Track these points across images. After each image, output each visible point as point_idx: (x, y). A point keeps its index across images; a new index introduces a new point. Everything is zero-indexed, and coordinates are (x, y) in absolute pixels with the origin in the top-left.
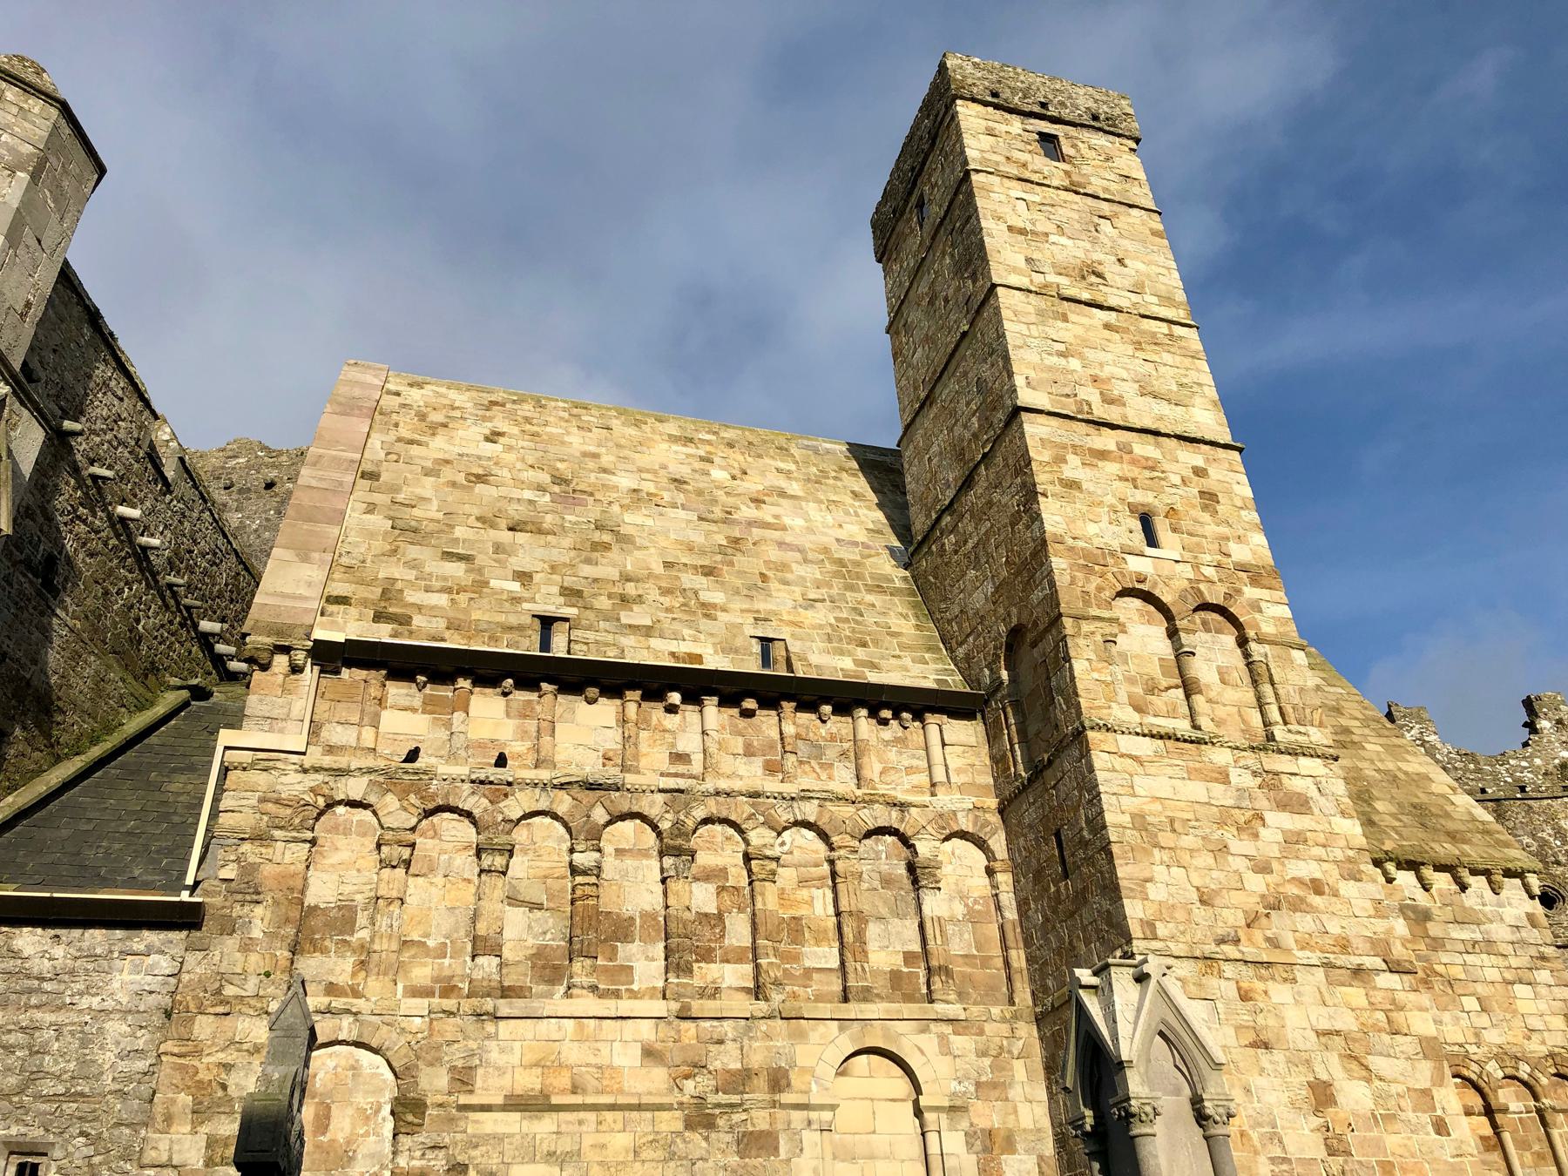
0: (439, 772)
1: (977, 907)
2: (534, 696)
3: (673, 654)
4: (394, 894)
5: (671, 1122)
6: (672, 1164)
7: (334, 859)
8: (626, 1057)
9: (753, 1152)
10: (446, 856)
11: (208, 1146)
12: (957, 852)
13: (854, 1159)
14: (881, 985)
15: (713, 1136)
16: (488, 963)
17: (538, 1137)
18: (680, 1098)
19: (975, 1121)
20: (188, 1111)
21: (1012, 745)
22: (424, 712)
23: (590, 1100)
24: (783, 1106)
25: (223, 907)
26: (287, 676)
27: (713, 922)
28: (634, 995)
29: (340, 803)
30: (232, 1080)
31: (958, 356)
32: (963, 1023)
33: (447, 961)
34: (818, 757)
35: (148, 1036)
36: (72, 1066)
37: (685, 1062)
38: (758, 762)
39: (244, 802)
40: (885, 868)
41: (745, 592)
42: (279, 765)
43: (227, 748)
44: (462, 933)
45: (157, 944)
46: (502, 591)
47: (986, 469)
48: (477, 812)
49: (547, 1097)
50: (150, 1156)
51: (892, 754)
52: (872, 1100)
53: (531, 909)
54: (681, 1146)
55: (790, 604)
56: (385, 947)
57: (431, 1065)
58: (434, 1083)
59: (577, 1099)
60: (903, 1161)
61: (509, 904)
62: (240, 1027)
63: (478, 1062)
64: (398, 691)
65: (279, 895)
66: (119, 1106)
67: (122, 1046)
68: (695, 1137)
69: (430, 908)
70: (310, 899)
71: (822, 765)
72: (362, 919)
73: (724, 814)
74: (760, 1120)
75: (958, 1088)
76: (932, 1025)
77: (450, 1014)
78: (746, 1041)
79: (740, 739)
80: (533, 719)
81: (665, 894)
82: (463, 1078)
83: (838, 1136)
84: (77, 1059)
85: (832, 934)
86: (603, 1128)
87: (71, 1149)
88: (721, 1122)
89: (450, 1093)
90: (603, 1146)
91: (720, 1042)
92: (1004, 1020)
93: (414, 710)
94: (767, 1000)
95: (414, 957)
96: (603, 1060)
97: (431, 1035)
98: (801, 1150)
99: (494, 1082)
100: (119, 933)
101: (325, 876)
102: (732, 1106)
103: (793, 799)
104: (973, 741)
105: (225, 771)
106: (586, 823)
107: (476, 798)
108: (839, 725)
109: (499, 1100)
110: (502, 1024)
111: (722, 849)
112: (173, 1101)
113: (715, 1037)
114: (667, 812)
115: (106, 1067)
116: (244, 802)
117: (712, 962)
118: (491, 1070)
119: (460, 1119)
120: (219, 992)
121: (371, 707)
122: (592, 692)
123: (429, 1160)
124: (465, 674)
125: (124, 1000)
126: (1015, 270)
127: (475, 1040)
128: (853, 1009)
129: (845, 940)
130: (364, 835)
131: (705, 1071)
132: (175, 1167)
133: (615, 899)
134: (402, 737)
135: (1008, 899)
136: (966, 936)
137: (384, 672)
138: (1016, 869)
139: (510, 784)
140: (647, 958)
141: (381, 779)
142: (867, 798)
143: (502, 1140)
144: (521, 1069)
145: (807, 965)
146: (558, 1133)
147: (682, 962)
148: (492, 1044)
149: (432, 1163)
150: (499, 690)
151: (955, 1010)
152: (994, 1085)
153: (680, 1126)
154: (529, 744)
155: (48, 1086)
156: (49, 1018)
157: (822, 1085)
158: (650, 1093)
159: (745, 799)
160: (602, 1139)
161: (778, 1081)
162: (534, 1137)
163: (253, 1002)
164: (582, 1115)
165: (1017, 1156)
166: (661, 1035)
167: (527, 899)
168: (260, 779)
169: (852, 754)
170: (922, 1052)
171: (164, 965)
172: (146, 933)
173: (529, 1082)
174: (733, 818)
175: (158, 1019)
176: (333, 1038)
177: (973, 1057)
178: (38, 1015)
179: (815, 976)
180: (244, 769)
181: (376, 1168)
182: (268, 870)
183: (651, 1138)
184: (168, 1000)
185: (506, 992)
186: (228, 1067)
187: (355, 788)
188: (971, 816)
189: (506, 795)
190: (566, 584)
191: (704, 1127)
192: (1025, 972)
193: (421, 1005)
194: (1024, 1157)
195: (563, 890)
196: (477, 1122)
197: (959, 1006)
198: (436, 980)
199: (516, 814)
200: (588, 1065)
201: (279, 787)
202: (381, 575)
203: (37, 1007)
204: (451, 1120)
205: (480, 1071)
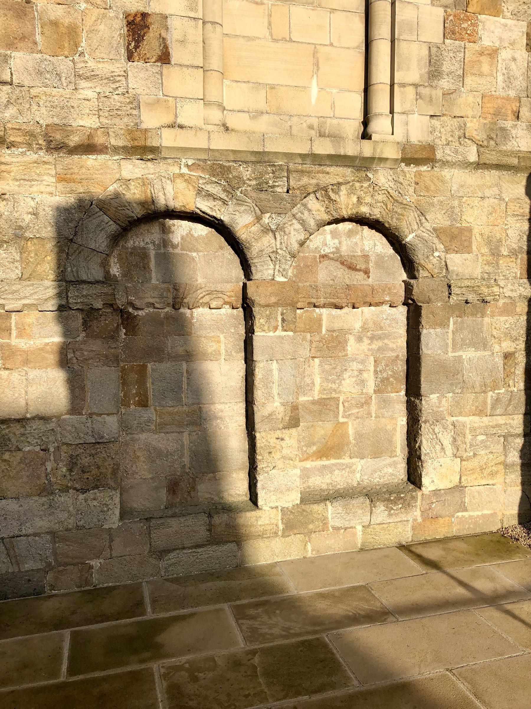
60: (333, 10)
165: (500, 19)
194: (510, 22)
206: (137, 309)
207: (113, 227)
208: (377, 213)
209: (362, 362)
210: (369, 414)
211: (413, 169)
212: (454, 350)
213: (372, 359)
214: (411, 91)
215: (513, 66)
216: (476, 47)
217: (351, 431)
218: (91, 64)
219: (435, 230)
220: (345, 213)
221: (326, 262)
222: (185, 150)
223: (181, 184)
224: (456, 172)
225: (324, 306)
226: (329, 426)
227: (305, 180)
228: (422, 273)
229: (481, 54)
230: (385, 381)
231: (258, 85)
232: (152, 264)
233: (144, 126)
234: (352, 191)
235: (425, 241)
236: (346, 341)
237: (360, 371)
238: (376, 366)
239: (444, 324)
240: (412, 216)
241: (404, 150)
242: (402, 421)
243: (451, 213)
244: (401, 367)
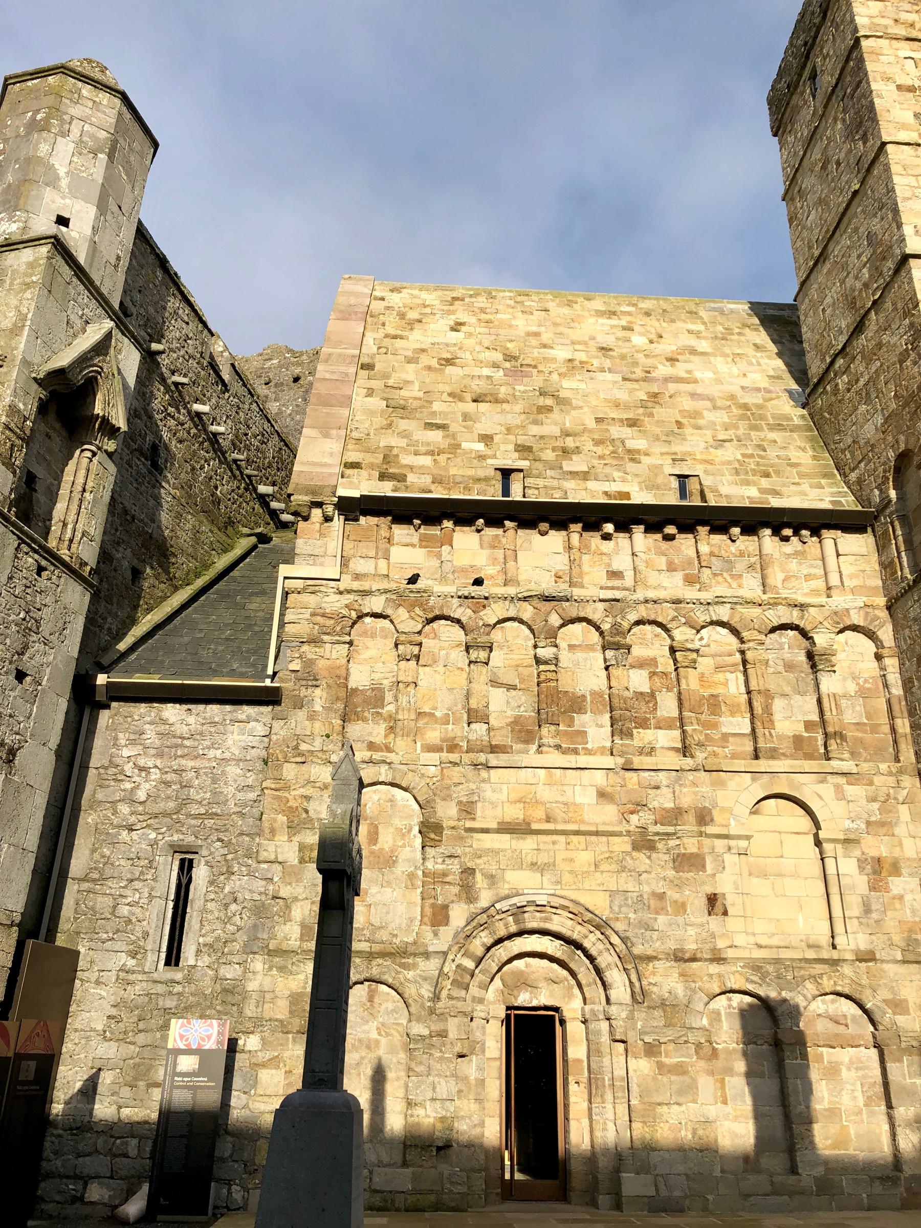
0: (435, 590)
2: (500, 531)
3: (606, 493)
4: (410, 679)
5: (622, 845)
6: (624, 874)
7: (366, 655)
8: (586, 797)
9: (686, 868)
11: (300, 851)
12: (850, 642)
13: (765, 875)
14: (785, 747)
15: (654, 855)
16: (479, 729)
18: (627, 828)
19: (866, 851)
20: (285, 827)
21: (899, 553)
23: (560, 827)
24: (707, 836)
25: (294, 690)
26: (322, 524)
27: (647, 699)
28: (589, 752)
29: (367, 615)
30: (311, 807)
31: (849, 213)
32: (856, 776)
33: (450, 727)
34: (729, 570)
35: (254, 777)
36: (208, 795)
37: (630, 802)
38: (679, 577)
39: (301, 616)
40: (787, 656)
41: (664, 438)
42: (322, 589)
43: (285, 578)
44: (460, 706)
45: (254, 715)
46: (471, 450)
47: (876, 314)
48: (464, 620)
49: (529, 824)
50: (263, 855)
51: (793, 565)
52: (780, 833)
53: (508, 690)
54: (630, 862)
55: (703, 445)
56: (406, 717)
57: (444, 800)
58: (447, 812)
60: (806, 878)
61: (492, 686)
62: (313, 772)
63: (477, 798)
64: (401, 532)
65: (330, 681)
66: (240, 822)
67: (238, 782)
68: (641, 856)
69: (436, 689)
70: (352, 684)
71: (732, 576)
72: (389, 697)
73: (652, 617)
74: (691, 845)
75: (851, 825)
76: (829, 777)
77: (455, 764)
78: (677, 788)
79: (664, 559)
80: (500, 549)
81: (609, 678)
82: (467, 809)
83: (752, 859)
84: (211, 791)
85: (744, 707)
86: (571, 847)
87: (213, 850)
88: (660, 846)
89: (459, 820)
90: (572, 860)
91: (657, 788)
92: (890, 774)
93: (413, 546)
94: (692, 757)
95: (427, 723)
96: (568, 798)
97: (442, 779)
98: (724, 868)
99: (489, 812)
100: (228, 708)
101: (360, 667)
102: (667, 834)
103: (709, 604)
104: (864, 551)
105: (286, 594)
106: (545, 625)
107: (463, 609)
108: (747, 543)
109: (494, 825)
110: (492, 771)
111: (652, 644)
112: (275, 820)
113: (652, 783)
114: (607, 616)
115: (230, 796)
116: (301, 616)
117: (648, 728)
119: (467, 837)
120: (296, 747)
121: (383, 545)
122: (544, 526)
123: (448, 865)
124: (448, 517)
125: (237, 753)
126: (904, 127)
127: (474, 783)
128: (763, 765)
129: (755, 712)
130: (386, 637)
131: (646, 809)
132: (280, 863)
133: (570, 682)
134: (406, 566)
135: (894, 678)
136: (858, 708)
137: (390, 518)
138: (902, 654)
139: (486, 598)
141: (394, 597)
142: (771, 601)
144: (508, 804)
146: (538, 850)
147: (624, 729)
148: (486, 786)
149: (450, 867)
150: (473, 528)
151: (848, 766)
152: (882, 824)
153: (628, 848)
154: (498, 568)
155: (194, 809)
156: (191, 764)
158: (604, 824)
159: (669, 605)
160: (569, 854)
161: (703, 817)
163: (320, 755)
164: (555, 837)
165: (901, 878)
166: (611, 781)
168: (311, 600)
169: (758, 566)
170: (820, 797)
171: (260, 729)
172: (245, 708)
173: (514, 813)
174: (660, 620)
175: (259, 765)
176: (375, 780)
177: (864, 802)
178: (183, 762)
179: (731, 739)
180: (299, 593)
181: (412, 869)
182: (321, 663)
183: (607, 855)
184: (264, 753)
185: (494, 749)
186: (308, 798)
187: (376, 604)
188: (862, 613)
189: (484, 607)
190: (519, 442)
192: (909, 737)
193: (434, 757)
195: (529, 676)
196: (479, 840)
197: (851, 763)
198: (443, 740)
200: (557, 802)
201: (323, 605)
202: (382, 444)
203: (182, 756)
204: (462, 838)
205: (479, 805)
206: (717, 1044)
207: (706, 999)
208: (846, 991)
209: (853, 1084)
210: (862, 1121)
211: (864, 964)
212: (910, 1078)
213: (859, 1083)
214: (855, 921)
215: (915, 903)
216: (890, 895)
217: (852, 1132)
218: (693, 919)
219: (884, 1000)
220: (828, 991)
221: (821, 1019)
222: (738, 959)
223: (738, 976)
224: (891, 965)
225: (823, 1046)
226: (838, 1126)
227: (802, 972)
228: (880, 1027)
229: (894, 898)
230: (869, 1098)
231: (770, 920)
232: (723, 1018)
233: (718, 947)
234: (830, 978)
235: (879, 1007)
236: (841, 1070)
237: (853, 1091)
238: (862, 1088)
239: (900, 1060)
240: (868, 992)
241: (856, 954)
242: (886, 1127)
243: (892, 990)
244: (880, 1089)
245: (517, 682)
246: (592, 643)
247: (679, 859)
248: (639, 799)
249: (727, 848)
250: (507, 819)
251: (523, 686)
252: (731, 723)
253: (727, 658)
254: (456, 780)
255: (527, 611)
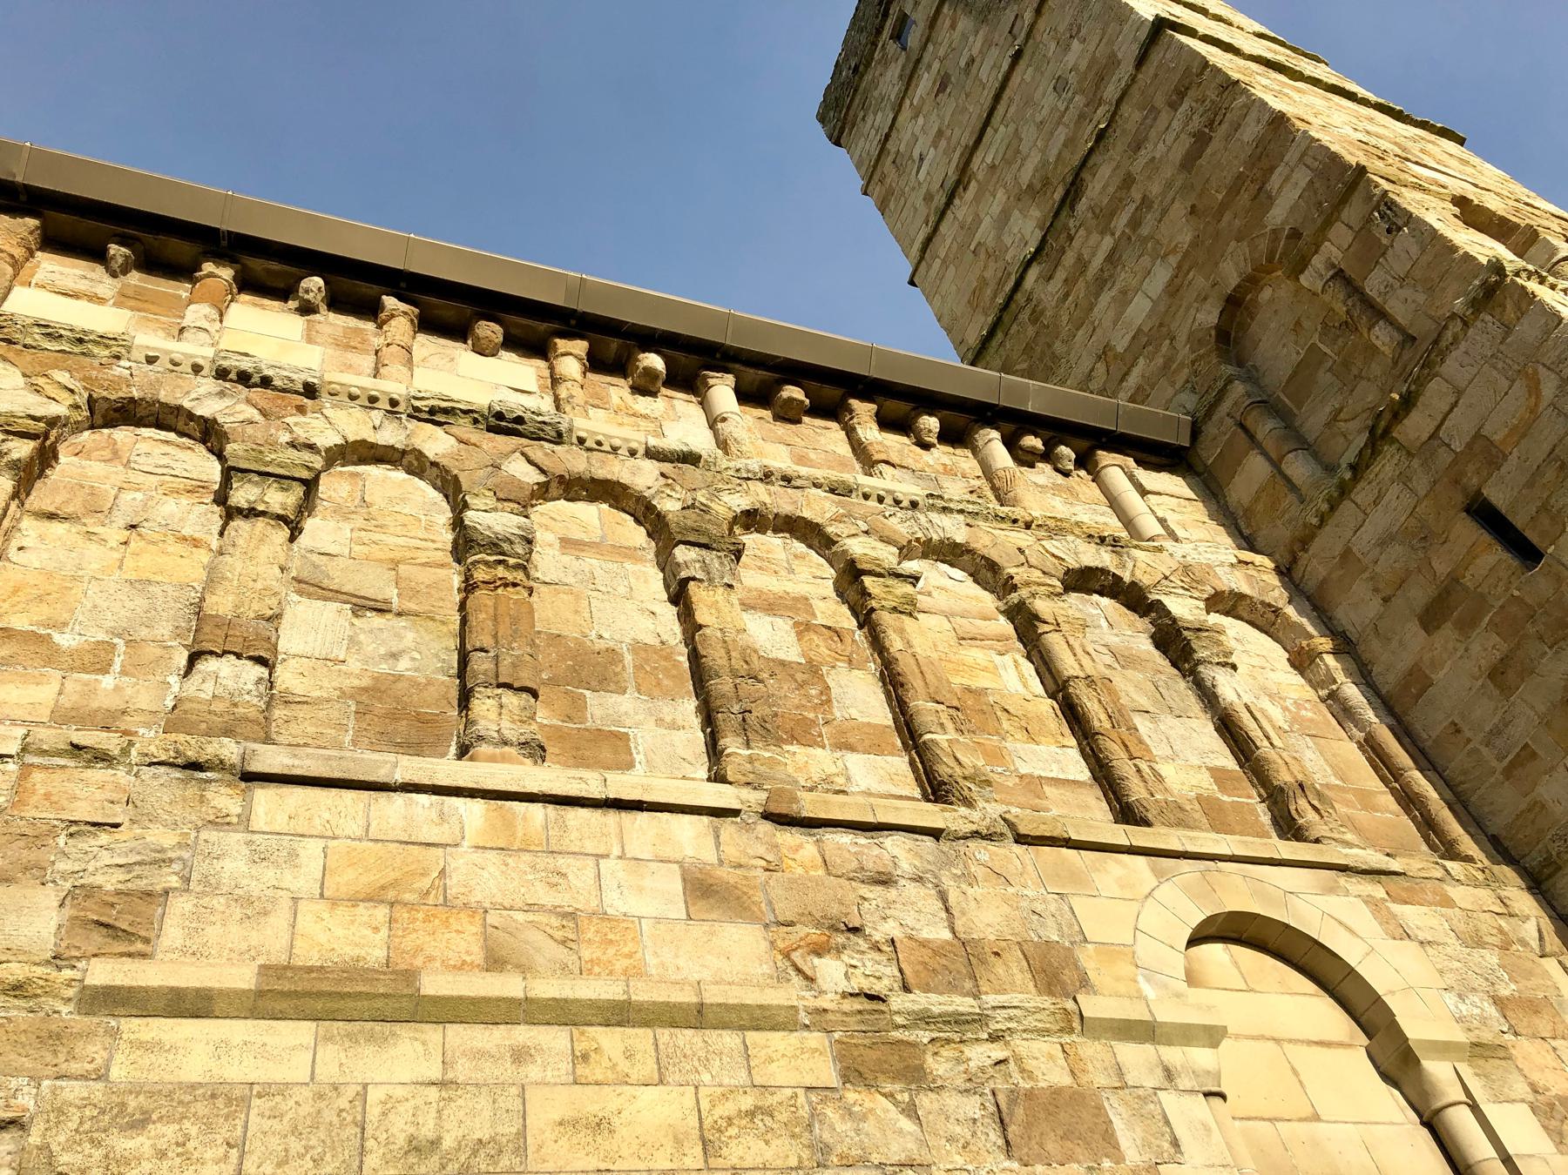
0: (137, 342)
1: (1303, 713)
2: (370, 326)
10: (139, 496)
15: (926, 1102)
17: (374, 1095)
22: (117, 305)
23: (546, 989)
27: (799, 677)
33: (107, 682)
37: (808, 916)
40: (1113, 640)
44: (164, 630)
49: (410, 976)
52: (1277, 1041)
54: (841, 1127)
59: (508, 986)
61: (300, 593)
63: (174, 881)
76: (1342, 880)
77: (102, 758)
78: (948, 883)
80: (366, 352)
88: (939, 1065)
90: (600, 1125)
94: (968, 803)
96: (579, 888)
98: (1175, 1143)
99: (226, 933)
102: (957, 1020)
103: (914, 505)
107: (227, 402)
109: (243, 978)
110: (264, 795)
111: (791, 571)
118: (218, 903)
119: (88, 1035)
133: (571, 617)
140: (660, 722)
143: (244, 1102)
144: (322, 906)
145: (1023, 771)
146: (441, 1084)
147: (751, 718)
150: (293, 304)
153: (828, 1074)
157: (1165, 986)
160: (591, 1102)
162: (363, 1095)
164: (523, 1034)
166: (731, 852)
167: (348, 588)
174: (807, 514)
179: (1049, 790)
183: (747, 1102)
191: (896, 1076)
195: (433, 586)
199: (328, 439)
200: (530, 908)
204: (54, 1038)
205: (180, 906)
245: (392, 593)
246: (630, 544)
247: (1020, 1112)
248: (835, 910)
249: (1159, 1072)
250: (307, 955)
251: (412, 606)
252: (1034, 752)
253: (979, 622)
254: (83, 812)
255: (435, 443)
